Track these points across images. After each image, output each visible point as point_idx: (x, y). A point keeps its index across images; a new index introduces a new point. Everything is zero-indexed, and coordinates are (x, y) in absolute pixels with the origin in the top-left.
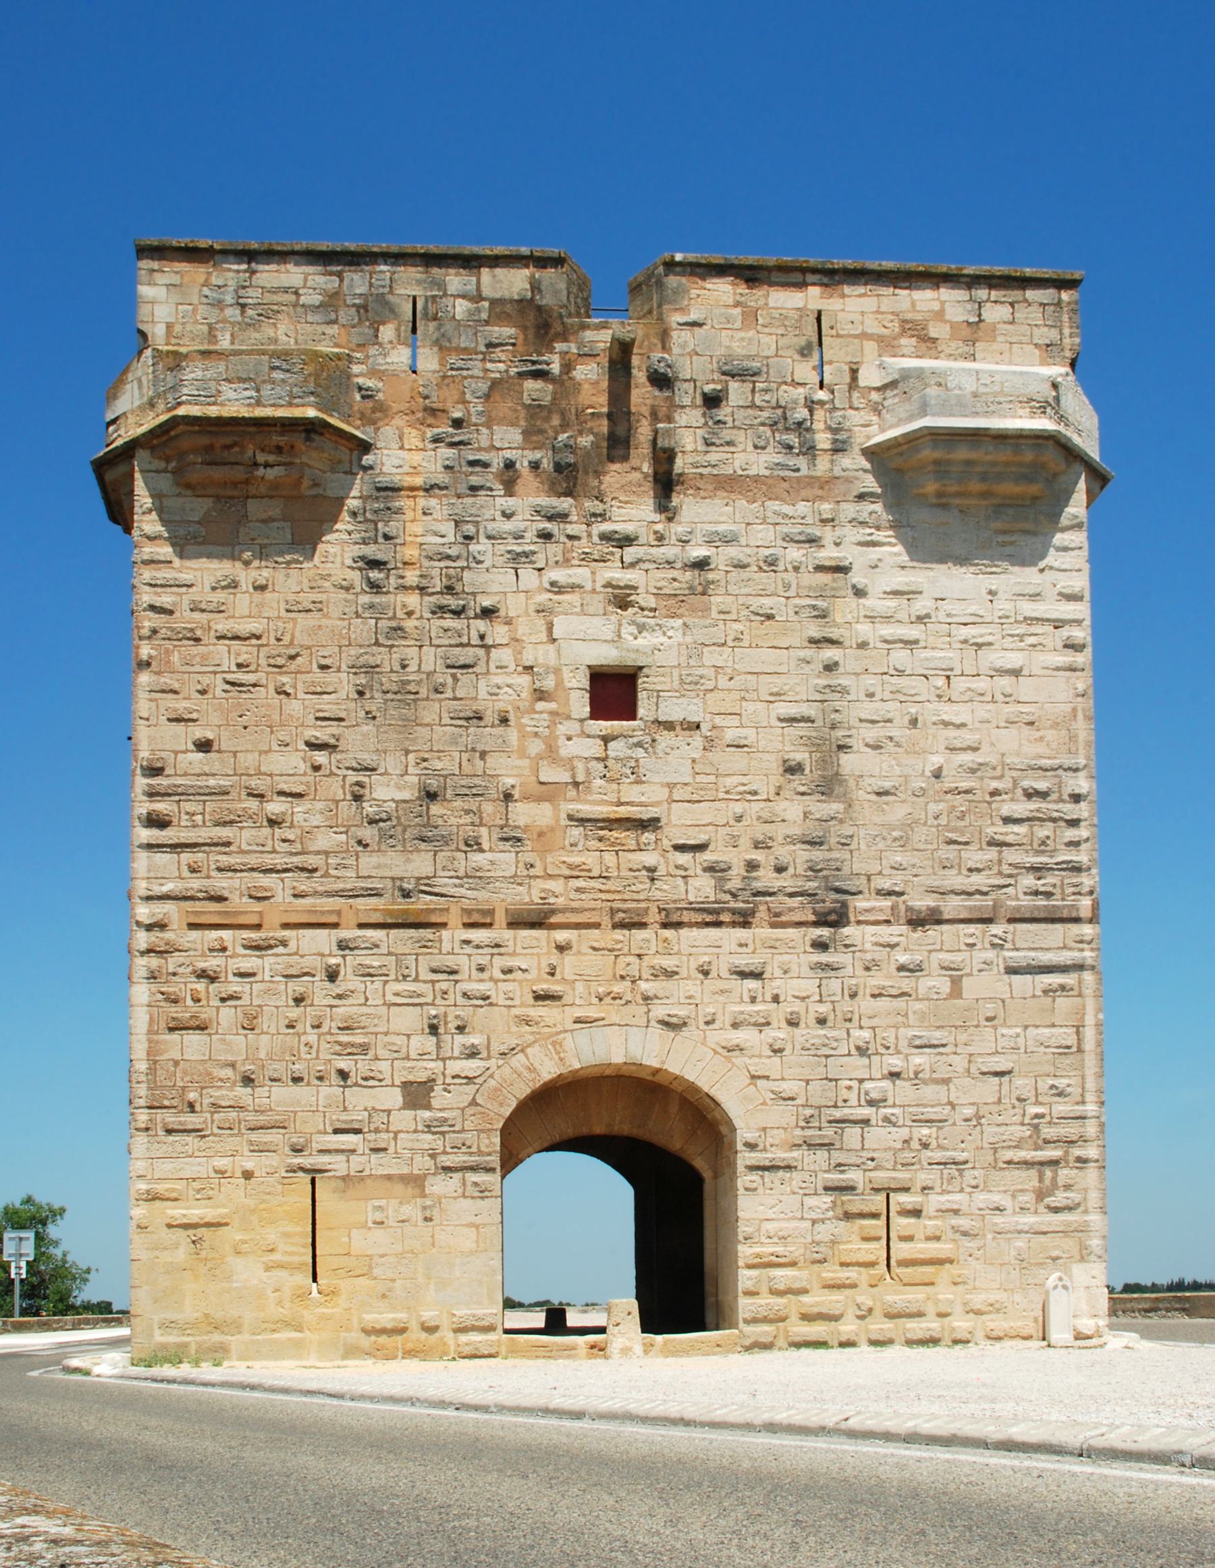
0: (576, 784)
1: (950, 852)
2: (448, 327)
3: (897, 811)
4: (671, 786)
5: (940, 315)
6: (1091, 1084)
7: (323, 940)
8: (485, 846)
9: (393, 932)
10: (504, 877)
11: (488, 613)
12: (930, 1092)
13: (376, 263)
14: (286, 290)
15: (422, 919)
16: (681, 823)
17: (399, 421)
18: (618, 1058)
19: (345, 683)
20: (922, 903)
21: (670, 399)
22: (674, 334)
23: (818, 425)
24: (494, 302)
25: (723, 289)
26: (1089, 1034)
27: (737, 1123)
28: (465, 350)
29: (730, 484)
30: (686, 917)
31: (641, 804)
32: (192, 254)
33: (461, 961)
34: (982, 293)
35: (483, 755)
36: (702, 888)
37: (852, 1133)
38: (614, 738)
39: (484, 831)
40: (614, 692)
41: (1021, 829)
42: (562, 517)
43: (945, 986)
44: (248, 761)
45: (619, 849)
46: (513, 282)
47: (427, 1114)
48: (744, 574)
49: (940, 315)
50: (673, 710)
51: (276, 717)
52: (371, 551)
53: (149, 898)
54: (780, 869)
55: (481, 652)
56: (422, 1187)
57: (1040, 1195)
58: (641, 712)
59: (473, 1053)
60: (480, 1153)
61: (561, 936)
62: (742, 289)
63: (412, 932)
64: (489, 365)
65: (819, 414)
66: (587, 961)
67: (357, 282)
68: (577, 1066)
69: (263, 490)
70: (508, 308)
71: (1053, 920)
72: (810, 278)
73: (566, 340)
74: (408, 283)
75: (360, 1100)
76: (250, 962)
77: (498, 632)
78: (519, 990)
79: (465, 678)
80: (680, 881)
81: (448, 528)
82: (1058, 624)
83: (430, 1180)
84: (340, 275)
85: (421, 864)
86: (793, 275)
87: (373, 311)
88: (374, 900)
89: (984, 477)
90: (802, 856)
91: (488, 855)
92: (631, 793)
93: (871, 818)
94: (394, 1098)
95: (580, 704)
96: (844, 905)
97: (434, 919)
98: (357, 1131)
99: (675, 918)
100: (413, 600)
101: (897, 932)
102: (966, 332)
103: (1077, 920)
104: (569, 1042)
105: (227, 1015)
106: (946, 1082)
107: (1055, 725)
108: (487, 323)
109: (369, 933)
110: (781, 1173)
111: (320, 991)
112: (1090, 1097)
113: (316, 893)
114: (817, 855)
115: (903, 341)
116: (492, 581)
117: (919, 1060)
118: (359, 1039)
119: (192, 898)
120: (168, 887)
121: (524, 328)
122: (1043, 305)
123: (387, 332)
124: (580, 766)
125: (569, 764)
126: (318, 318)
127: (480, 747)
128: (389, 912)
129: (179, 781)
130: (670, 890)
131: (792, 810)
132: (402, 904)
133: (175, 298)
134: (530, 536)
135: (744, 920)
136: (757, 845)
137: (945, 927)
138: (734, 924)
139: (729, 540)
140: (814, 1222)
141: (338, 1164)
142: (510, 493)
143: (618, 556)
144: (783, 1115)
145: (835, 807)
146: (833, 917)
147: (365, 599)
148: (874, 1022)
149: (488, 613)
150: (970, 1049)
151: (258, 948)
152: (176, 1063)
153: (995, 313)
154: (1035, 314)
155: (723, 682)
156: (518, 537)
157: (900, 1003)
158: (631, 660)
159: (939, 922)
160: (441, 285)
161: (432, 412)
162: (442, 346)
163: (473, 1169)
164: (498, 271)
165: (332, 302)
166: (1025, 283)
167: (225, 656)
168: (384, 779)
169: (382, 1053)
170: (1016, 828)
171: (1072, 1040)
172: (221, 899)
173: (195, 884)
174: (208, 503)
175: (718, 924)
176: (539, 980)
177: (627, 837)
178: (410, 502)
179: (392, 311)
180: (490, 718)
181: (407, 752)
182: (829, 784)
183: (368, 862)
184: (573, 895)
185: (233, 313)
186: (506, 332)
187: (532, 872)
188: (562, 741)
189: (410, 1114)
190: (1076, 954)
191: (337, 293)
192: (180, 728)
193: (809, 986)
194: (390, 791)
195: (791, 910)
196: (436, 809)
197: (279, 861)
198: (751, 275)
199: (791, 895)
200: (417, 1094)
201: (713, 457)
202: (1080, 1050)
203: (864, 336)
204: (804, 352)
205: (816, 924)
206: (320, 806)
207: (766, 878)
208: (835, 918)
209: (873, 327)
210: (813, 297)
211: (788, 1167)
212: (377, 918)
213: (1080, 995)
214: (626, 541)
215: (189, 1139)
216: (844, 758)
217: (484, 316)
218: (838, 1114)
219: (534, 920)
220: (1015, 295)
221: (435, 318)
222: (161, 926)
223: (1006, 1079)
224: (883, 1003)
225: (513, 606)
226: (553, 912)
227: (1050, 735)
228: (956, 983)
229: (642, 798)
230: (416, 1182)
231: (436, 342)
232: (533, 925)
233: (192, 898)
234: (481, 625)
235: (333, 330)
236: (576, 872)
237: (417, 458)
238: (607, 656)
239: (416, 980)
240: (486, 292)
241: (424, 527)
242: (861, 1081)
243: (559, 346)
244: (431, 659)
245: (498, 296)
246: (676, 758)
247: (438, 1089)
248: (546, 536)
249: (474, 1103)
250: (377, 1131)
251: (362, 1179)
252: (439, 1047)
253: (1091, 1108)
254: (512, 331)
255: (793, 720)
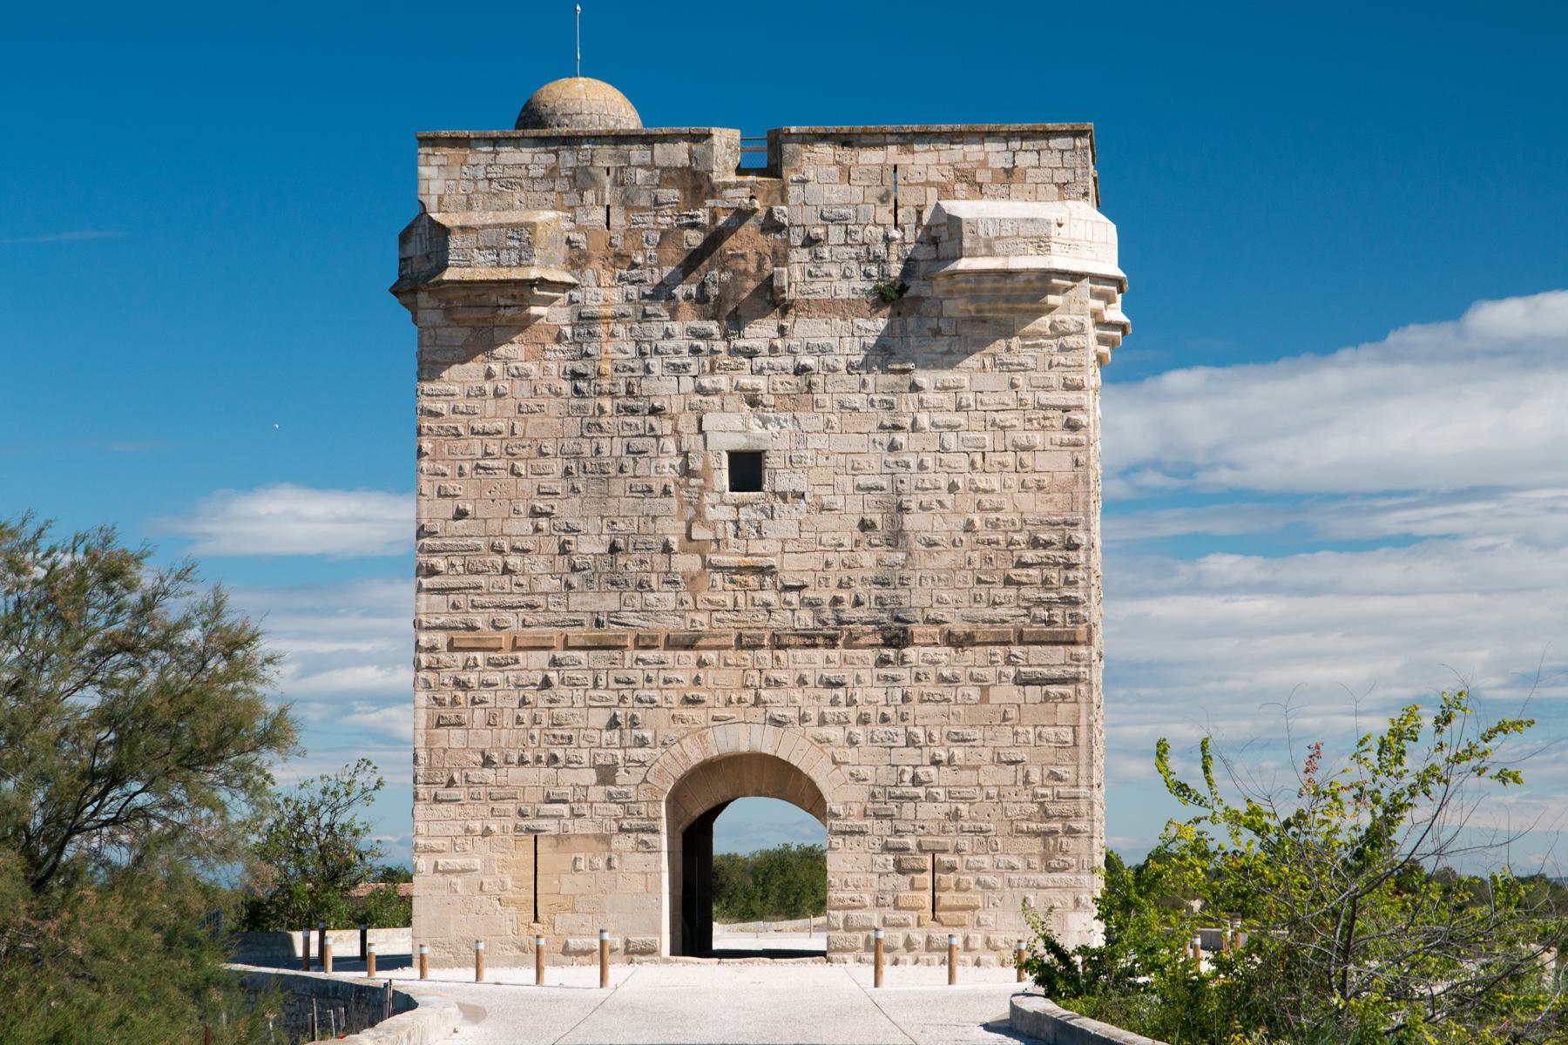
0: (717, 541)
1: (981, 590)
2: (632, 190)
3: (946, 559)
4: (784, 541)
5: (984, 164)
6: (1083, 772)
7: (543, 657)
8: (655, 586)
9: (592, 653)
10: (665, 609)
11: (654, 411)
12: (965, 776)
13: (580, 143)
14: (520, 166)
15: (612, 643)
16: (792, 568)
17: (596, 264)
18: (744, 748)
19: (557, 466)
20: (960, 627)
21: (787, 241)
22: (790, 189)
23: (894, 257)
24: (663, 169)
25: (825, 151)
26: (1083, 731)
27: (827, 798)
28: (644, 209)
29: (830, 307)
30: (793, 641)
31: (762, 555)
32: (454, 142)
33: (638, 675)
34: (1016, 144)
35: (654, 518)
36: (806, 618)
37: (909, 806)
38: (744, 505)
39: (654, 577)
40: (747, 470)
41: (1034, 572)
42: (706, 336)
43: (975, 693)
44: (494, 525)
45: (745, 587)
46: (679, 153)
47: (612, 789)
48: (838, 377)
49: (984, 164)
50: (783, 484)
51: (513, 492)
52: (579, 366)
53: (428, 628)
54: (858, 603)
55: (653, 441)
56: (609, 844)
57: (1046, 858)
58: (765, 487)
59: (642, 743)
60: (649, 818)
61: (706, 655)
62: (840, 151)
63: (605, 653)
64: (660, 219)
65: (894, 248)
66: (723, 674)
67: (568, 158)
68: (716, 753)
69: (504, 322)
70: (673, 174)
71: (1057, 643)
72: (889, 139)
73: (713, 197)
74: (604, 156)
75: (568, 776)
76: (495, 676)
77: (666, 426)
78: (675, 697)
79: (642, 462)
80: (789, 614)
81: (631, 348)
82: (1066, 410)
83: (615, 839)
84: (556, 153)
85: (611, 602)
86: (877, 140)
87: (581, 180)
88: (579, 628)
89: (1007, 300)
90: (876, 591)
91: (657, 595)
92: (757, 546)
93: (927, 564)
94: (590, 776)
95: (723, 478)
96: (905, 630)
97: (620, 643)
98: (565, 802)
99: (784, 641)
100: (607, 403)
101: (943, 653)
102: (1003, 176)
103: (1074, 643)
104: (710, 736)
105: (479, 714)
106: (976, 768)
107: (1062, 490)
108: (658, 186)
109: (576, 654)
110: (857, 837)
111: (540, 699)
112: (1082, 782)
113: (540, 624)
114: (885, 593)
115: (957, 186)
116: (664, 389)
117: (959, 752)
118: (566, 733)
119: (456, 628)
120: (443, 619)
121: (683, 189)
122: (1062, 151)
123: (589, 196)
124: (720, 526)
125: (713, 526)
126: (542, 187)
127: (652, 513)
128: (589, 638)
129: (448, 541)
130: (782, 620)
131: (868, 558)
132: (597, 633)
133: (444, 175)
134: (685, 351)
135: (832, 642)
136: (840, 586)
137: (977, 649)
138: (826, 646)
139: (823, 350)
140: (880, 875)
141: (551, 826)
142: (673, 318)
143: (747, 366)
144: (859, 793)
145: (901, 556)
146: (895, 641)
147: (574, 402)
148: (925, 721)
149: (654, 411)
150: (994, 743)
151: (496, 665)
152: (445, 751)
153: (1026, 160)
154: (1056, 160)
155: (822, 461)
156: (677, 352)
157: (943, 707)
158: (755, 446)
159: (974, 645)
160: (627, 158)
161: (620, 257)
162: (628, 205)
163: (643, 830)
164: (666, 145)
165: (552, 173)
166: (1048, 135)
167: (477, 446)
168: (588, 538)
169: (583, 743)
170: (1031, 571)
171: (1070, 738)
172: (474, 628)
173: (458, 618)
174: (467, 332)
175: (815, 646)
176: (690, 689)
177: (752, 580)
178: (604, 328)
179: (593, 179)
180: (658, 489)
181: (602, 518)
182: (896, 538)
183: (575, 600)
184: (715, 624)
185: (483, 185)
186: (671, 194)
187: (686, 607)
188: (709, 509)
189: (601, 788)
190: (1073, 670)
191: (554, 169)
192: (448, 501)
193: (878, 694)
194: (589, 547)
195: (867, 634)
196: (621, 560)
197: (515, 600)
198: (845, 141)
199: (867, 623)
200: (606, 774)
201: (818, 286)
202: (1075, 745)
203: (928, 184)
204: (883, 200)
205: (885, 645)
206: (542, 558)
207: (849, 612)
208: (897, 638)
209: (934, 176)
210: (893, 153)
211: (862, 833)
212: (580, 642)
213: (1076, 702)
214: (751, 354)
215: (452, 806)
216: (906, 518)
217: (656, 181)
218: (898, 792)
219: (689, 644)
220: (1041, 144)
221: (622, 184)
222: (433, 649)
223: (1020, 767)
224: (929, 708)
225: (674, 405)
226: (700, 637)
227: (1058, 497)
228: (985, 690)
229: (765, 550)
230: (605, 839)
231: (623, 203)
232: (687, 647)
233: (456, 628)
234: (652, 420)
235: (552, 196)
236: (717, 607)
237: (608, 292)
238: (740, 443)
239: (607, 688)
240: (659, 161)
241: (615, 347)
242: (915, 767)
243: (709, 203)
244: (618, 447)
245: (666, 164)
246: (788, 518)
247: (621, 771)
248: (695, 351)
249: (645, 781)
250: (579, 801)
251: (568, 838)
252: (621, 738)
253: (1083, 790)
254: (677, 193)
255: (869, 489)
